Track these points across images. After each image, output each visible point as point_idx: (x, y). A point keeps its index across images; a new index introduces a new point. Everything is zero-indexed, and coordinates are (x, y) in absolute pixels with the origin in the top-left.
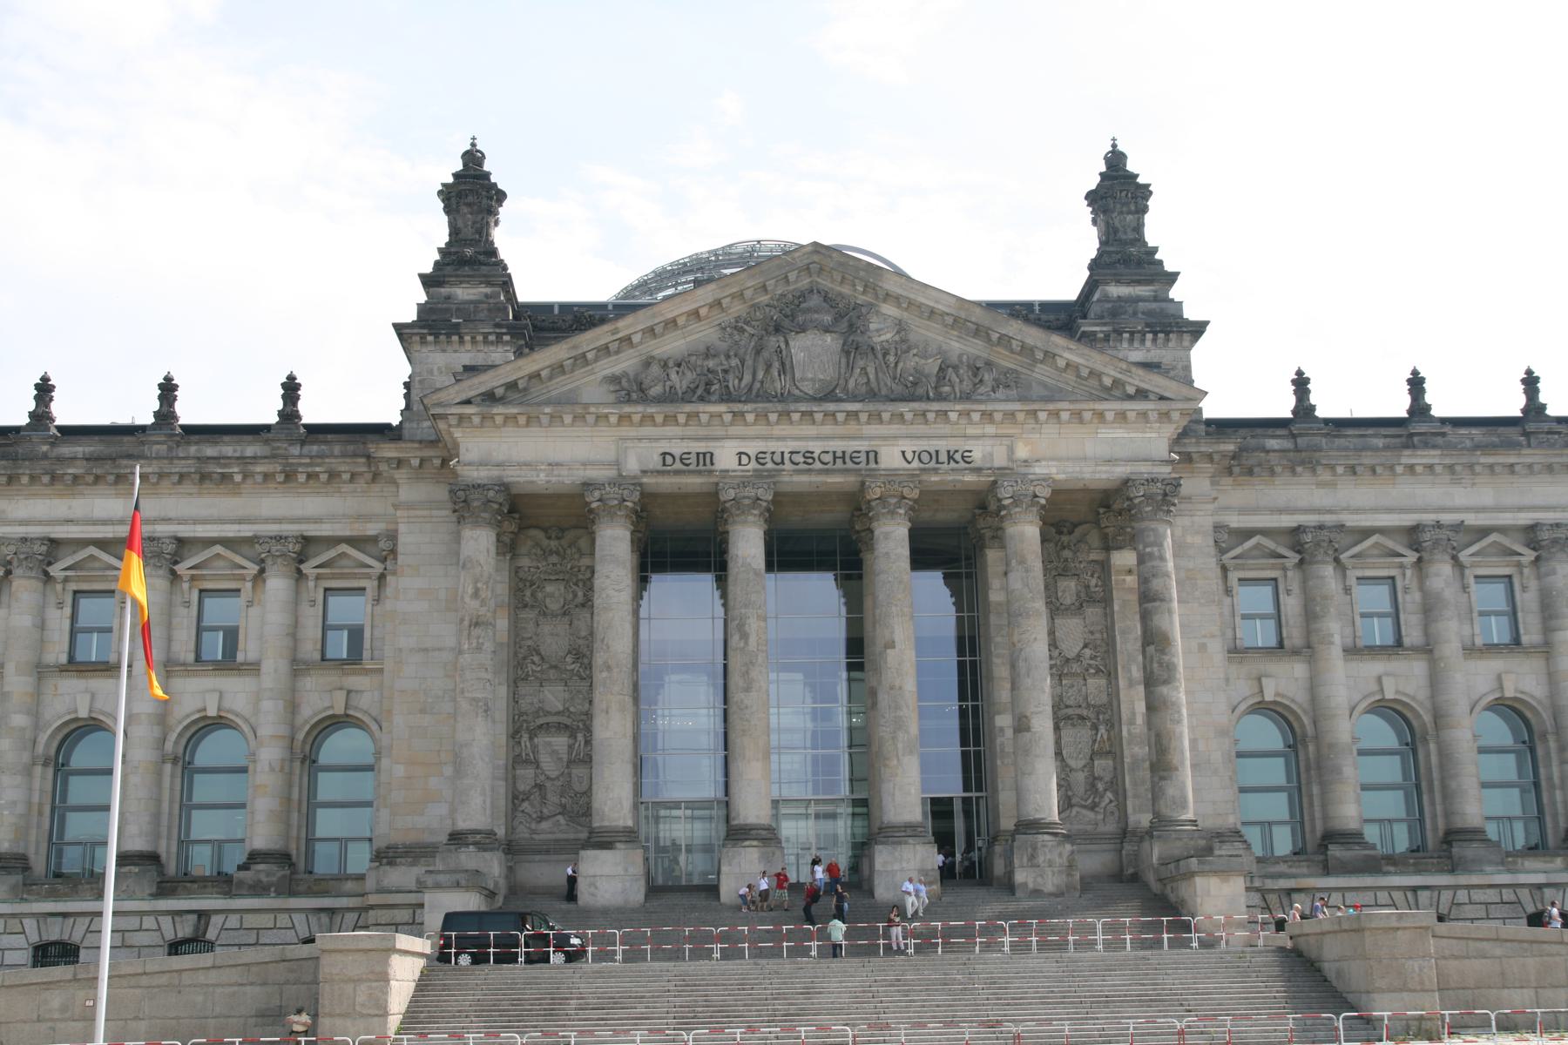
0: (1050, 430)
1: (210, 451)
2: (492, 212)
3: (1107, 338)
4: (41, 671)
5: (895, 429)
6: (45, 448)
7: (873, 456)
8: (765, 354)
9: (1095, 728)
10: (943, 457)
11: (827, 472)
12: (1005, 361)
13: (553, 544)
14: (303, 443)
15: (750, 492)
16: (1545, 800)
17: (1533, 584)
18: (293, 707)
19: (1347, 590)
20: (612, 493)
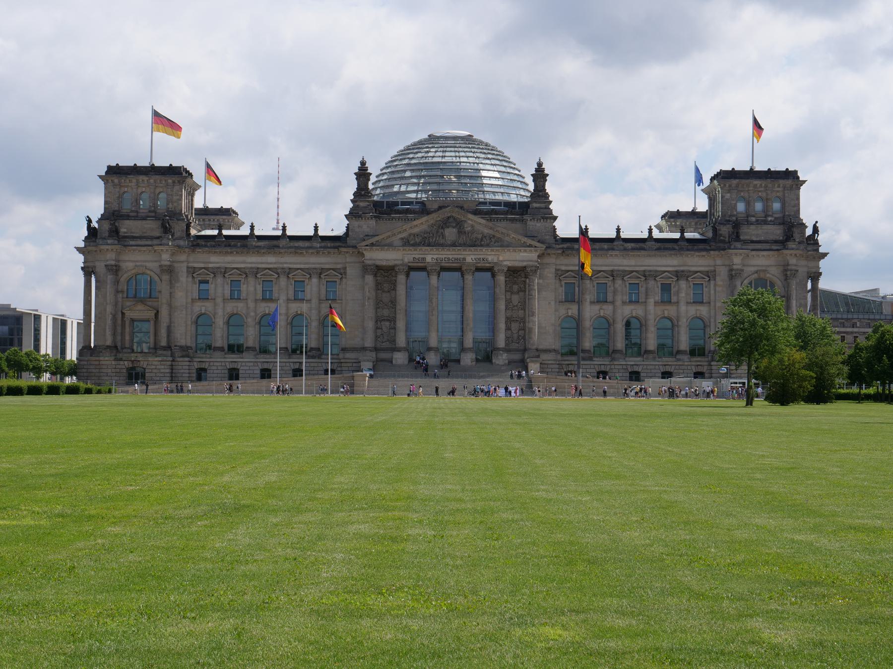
0: (508, 253)
1: (297, 244)
2: (369, 180)
3: (531, 220)
4: (256, 300)
5: (470, 253)
7: (464, 259)
8: (439, 234)
9: (520, 323)
10: (482, 260)
11: (453, 263)
12: (498, 235)
13: (386, 274)
15: (434, 268)
17: (644, 286)
18: (320, 312)
19: (594, 287)
20: (401, 267)
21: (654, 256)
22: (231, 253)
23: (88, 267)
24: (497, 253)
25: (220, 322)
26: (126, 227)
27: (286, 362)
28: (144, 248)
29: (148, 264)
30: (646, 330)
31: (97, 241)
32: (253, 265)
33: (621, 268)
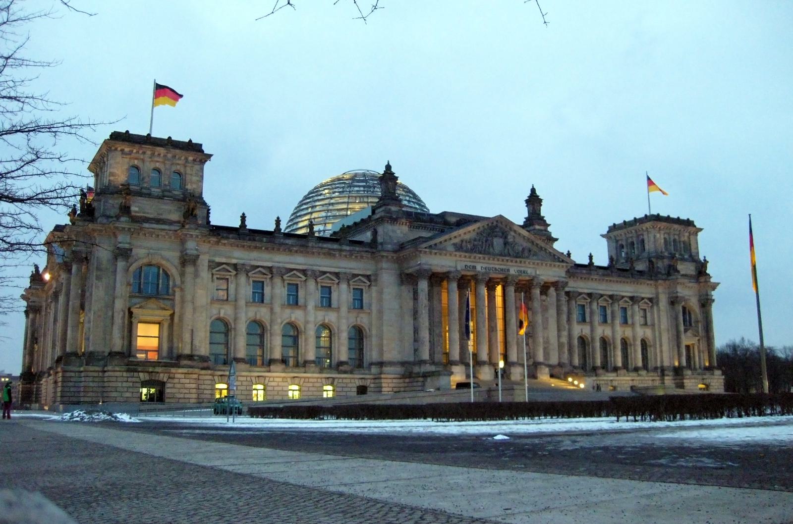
1: (325, 246)
4: (283, 306)
5: (515, 264)
6: (282, 240)
7: (508, 270)
8: (489, 242)
14: (349, 246)
16: (609, 359)
21: (620, 282)
22: (261, 248)
23: (80, 252)
24: (537, 267)
25: (242, 327)
26: (138, 207)
27: (318, 378)
28: (163, 233)
29: (162, 252)
30: (614, 348)
31: (99, 220)
32: (281, 265)
33: (597, 292)
